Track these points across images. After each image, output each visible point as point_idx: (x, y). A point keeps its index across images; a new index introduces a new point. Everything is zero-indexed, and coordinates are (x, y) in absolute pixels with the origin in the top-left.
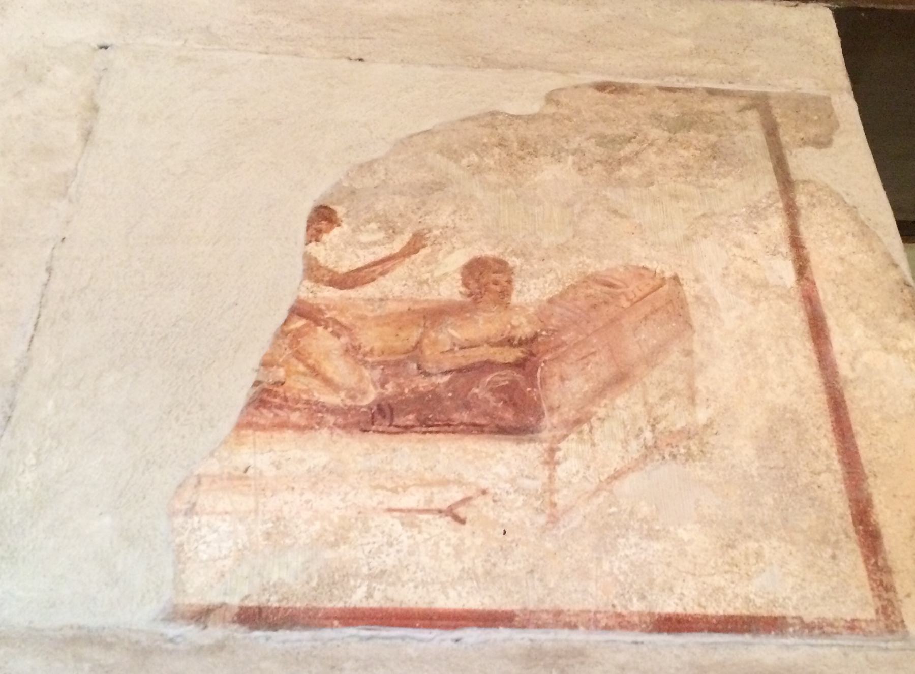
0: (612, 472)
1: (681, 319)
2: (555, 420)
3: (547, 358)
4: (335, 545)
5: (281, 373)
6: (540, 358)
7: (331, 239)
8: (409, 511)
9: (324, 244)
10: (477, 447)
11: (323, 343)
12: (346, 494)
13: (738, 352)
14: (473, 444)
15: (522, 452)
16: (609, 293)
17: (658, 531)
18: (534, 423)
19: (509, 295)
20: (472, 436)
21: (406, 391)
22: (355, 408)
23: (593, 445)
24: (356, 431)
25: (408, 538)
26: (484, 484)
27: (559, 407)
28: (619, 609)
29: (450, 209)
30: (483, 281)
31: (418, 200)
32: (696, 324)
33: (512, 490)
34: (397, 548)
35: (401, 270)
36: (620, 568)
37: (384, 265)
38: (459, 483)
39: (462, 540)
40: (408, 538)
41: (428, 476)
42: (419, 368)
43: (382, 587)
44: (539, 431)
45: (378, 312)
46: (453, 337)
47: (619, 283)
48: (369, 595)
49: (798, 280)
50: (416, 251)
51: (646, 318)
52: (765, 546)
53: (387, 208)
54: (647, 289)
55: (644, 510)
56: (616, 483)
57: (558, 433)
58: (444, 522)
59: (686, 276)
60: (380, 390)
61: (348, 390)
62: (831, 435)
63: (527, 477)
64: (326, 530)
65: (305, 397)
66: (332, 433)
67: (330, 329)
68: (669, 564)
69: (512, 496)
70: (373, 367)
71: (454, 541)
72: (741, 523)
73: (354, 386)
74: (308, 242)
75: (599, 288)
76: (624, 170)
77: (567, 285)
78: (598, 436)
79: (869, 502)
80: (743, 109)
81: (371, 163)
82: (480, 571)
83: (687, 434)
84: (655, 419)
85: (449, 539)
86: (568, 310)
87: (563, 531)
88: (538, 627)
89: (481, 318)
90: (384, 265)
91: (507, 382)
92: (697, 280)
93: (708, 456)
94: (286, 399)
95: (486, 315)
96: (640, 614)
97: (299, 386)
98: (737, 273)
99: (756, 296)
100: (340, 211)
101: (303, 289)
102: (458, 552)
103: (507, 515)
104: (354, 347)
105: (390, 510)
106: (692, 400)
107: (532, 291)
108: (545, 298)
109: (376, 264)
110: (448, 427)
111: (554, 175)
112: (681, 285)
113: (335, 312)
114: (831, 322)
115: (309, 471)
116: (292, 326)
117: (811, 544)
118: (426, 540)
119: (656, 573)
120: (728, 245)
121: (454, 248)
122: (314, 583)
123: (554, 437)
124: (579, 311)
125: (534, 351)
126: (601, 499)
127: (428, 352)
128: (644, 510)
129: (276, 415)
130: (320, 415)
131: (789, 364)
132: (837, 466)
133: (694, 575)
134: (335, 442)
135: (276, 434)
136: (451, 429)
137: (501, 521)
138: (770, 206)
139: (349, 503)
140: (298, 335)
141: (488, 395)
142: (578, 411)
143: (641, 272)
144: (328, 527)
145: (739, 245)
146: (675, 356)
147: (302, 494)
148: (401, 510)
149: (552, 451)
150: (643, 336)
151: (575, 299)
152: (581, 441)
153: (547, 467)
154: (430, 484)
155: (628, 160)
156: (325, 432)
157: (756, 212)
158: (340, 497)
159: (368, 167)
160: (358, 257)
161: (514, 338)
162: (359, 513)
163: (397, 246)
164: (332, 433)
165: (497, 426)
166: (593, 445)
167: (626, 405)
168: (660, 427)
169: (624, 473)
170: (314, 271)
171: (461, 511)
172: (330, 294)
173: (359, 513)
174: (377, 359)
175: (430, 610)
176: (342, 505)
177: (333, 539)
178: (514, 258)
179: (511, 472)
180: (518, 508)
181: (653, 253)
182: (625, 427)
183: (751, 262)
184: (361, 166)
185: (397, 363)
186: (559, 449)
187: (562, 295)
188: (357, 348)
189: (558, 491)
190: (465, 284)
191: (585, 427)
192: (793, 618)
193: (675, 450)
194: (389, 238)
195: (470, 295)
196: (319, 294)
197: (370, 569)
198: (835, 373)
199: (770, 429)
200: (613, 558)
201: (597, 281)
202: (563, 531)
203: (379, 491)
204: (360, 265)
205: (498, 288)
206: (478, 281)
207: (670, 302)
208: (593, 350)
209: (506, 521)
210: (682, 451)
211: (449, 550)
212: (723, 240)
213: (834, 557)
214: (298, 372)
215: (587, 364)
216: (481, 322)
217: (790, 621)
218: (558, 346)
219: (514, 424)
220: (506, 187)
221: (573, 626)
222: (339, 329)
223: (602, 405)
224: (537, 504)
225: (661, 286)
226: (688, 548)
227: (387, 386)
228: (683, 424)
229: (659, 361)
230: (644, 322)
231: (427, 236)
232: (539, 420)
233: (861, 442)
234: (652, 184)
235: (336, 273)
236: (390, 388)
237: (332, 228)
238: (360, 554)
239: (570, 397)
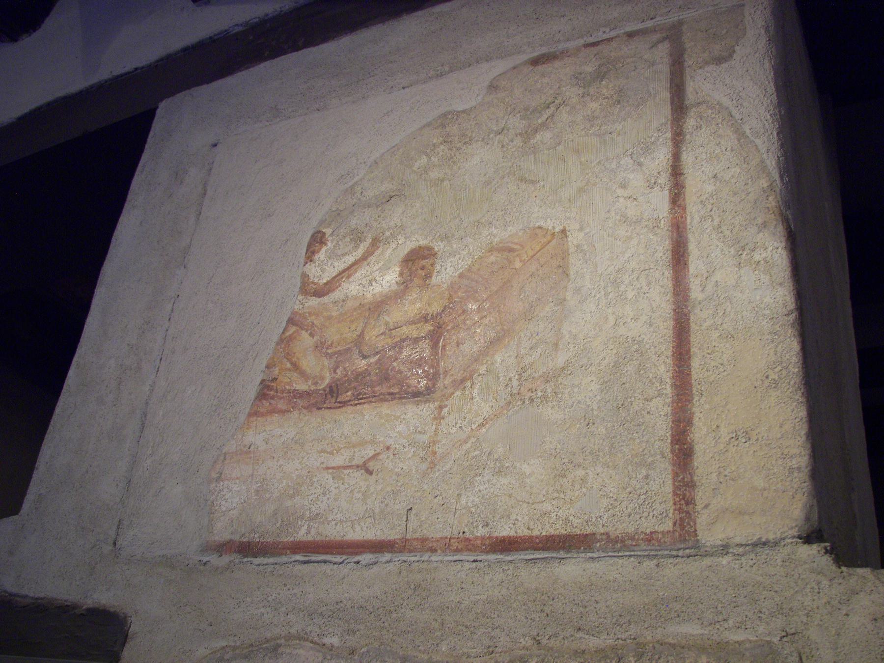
2: (448, 381)
3: (449, 328)
4: (292, 497)
8: (339, 467)
12: (303, 458)
13: (603, 293)
24: (314, 409)
26: (390, 442)
28: (467, 535)
29: (401, 211)
39: (368, 487)
41: (354, 439)
43: (316, 526)
48: (308, 532)
49: (671, 209)
54: (538, 247)
58: (358, 474)
59: (573, 226)
60: (333, 375)
62: (669, 361)
63: (420, 432)
65: (288, 387)
68: (510, 496)
76: (538, 137)
79: (690, 422)
80: (654, 45)
82: (377, 511)
85: (361, 487)
87: (437, 474)
88: (410, 551)
92: (581, 229)
93: (560, 396)
96: (483, 538)
98: (616, 214)
99: (629, 234)
100: (328, 231)
102: (365, 495)
103: (401, 465)
104: (321, 343)
109: (344, 271)
112: (566, 237)
113: (314, 317)
114: (692, 247)
115: (283, 443)
117: (630, 467)
118: (346, 489)
122: (278, 525)
126: (469, 445)
128: (500, 450)
132: (669, 390)
137: (396, 470)
140: (291, 339)
145: (623, 186)
148: (333, 468)
149: (441, 408)
154: (354, 446)
155: (544, 126)
156: (296, 413)
157: (647, 149)
168: (525, 375)
171: (371, 465)
175: (342, 541)
178: (440, 243)
186: (446, 406)
189: (439, 441)
191: (468, 384)
192: (602, 534)
196: (306, 305)
198: (686, 298)
202: (437, 474)
204: (334, 274)
210: (540, 394)
211: (360, 495)
213: (647, 477)
217: (598, 537)
220: (443, 180)
221: (433, 550)
224: (423, 454)
225: (549, 242)
226: (528, 480)
227: (338, 371)
228: (545, 370)
233: (695, 363)
234: (559, 144)
237: (321, 249)
238: (306, 503)
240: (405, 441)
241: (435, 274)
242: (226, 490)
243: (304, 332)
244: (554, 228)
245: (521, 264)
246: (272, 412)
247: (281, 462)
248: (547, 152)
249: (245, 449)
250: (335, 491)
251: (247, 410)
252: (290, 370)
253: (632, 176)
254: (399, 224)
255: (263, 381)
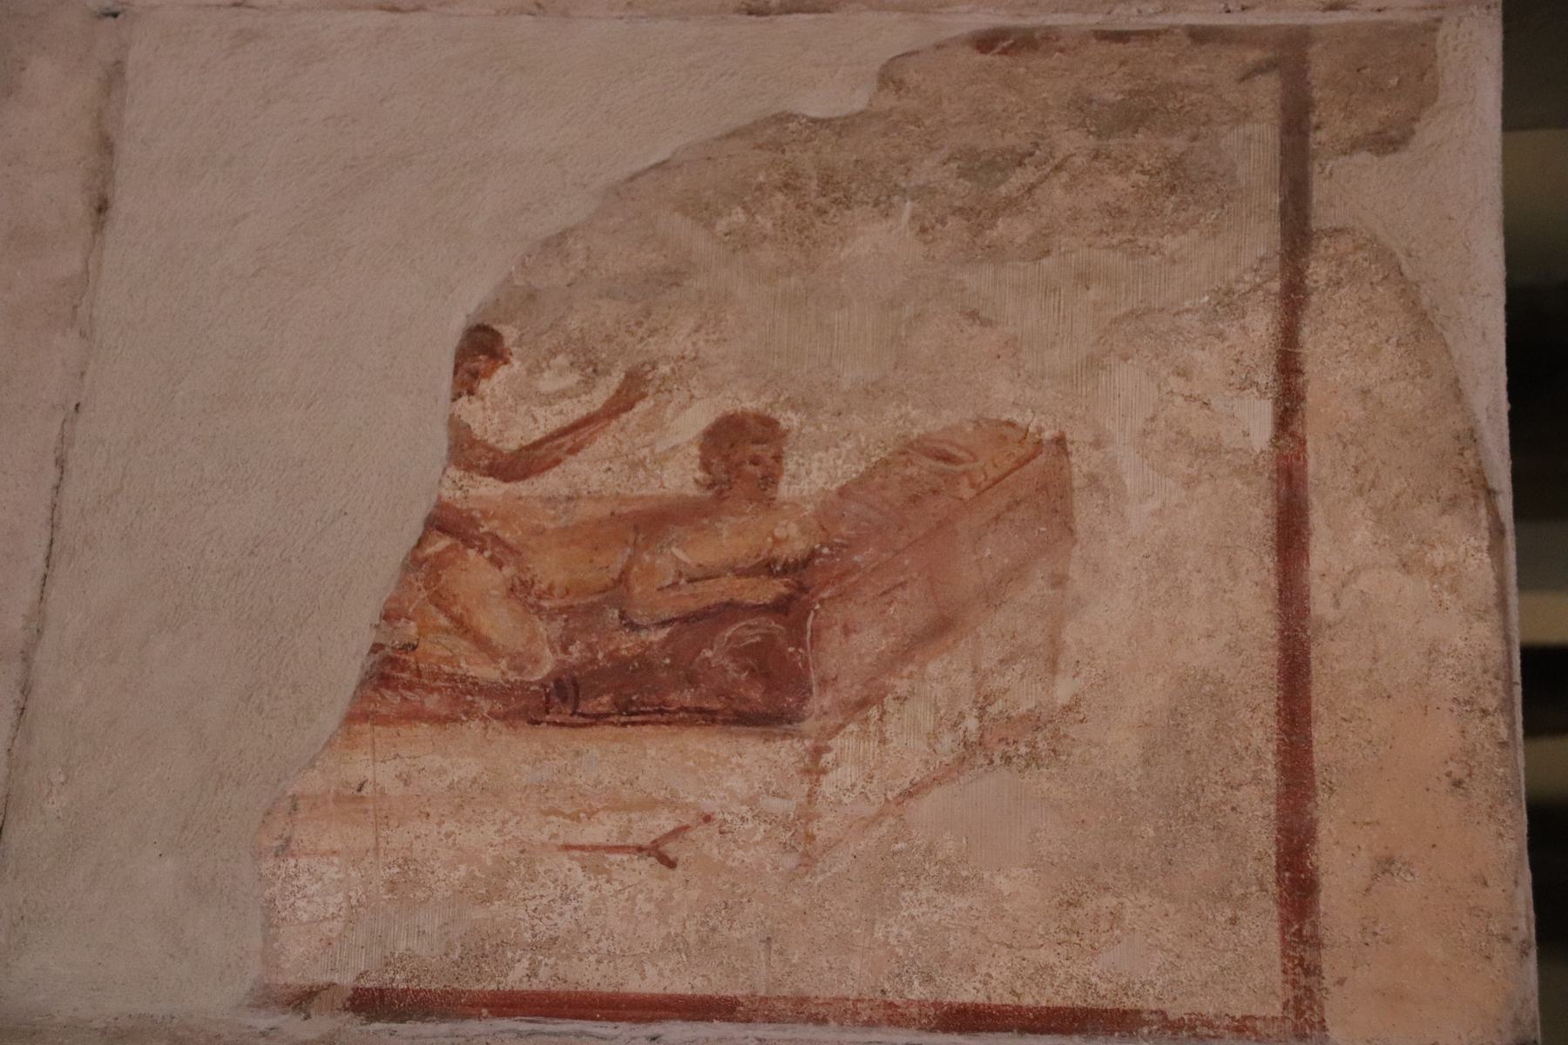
0: (907, 785)
1: (1057, 519)
2: (826, 702)
3: (825, 595)
4: (486, 900)
5: (412, 629)
6: (813, 596)
7: (493, 390)
8: (595, 848)
9: (482, 399)
10: (702, 747)
11: (477, 578)
12: (504, 822)
13: (1145, 578)
14: (697, 742)
15: (770, 755)
16: (942, 474)
17: (967, 878)
18: (794, 706)
19: (775, 483)
20: (696, 729)
21: (600, 656)
22: (524, 686)
23: (883, 741)
24: (522, 723)
25: (591, 889)
26: (708, 806)
27: (835, 679)
29: (691, 323)
30: (736, 458)
31: (638, 306)
32: (1081, 523)
33: (749, 816)
34: (574, 903)
35: (603, 443)
36: (900, 935)
37: (575, 435)
38: (672, 803)
40: (591, 889)
41: (626, 793)
42: (622, 617)
44: (802, 720)
45: (562, 522)
46: (678, 561)
47: (961, 454)
50: (631, 406)
51: (997, 518)
52: (1128, 904)
53: (586, 325)
54: (1008, 464)
55: (949, 846)
56: (912, 803)
57: (831, 722)
58: (645, 865)
59: (1078, 436)
60: (561, 656)
61: (513, 657)
63: (775, 794)
64: (474, 878)
65: (447, 669)
66: (486, 728)
67: (487, 554)
68: (974, 931)
69: (749, 826)
70: (551, 617)
71: (657, 894)
72: (1096, 867)
73: (521, 649)
74: (456, 397)
75: (928, 462)
77: (874, 460)
78: (890, 729)
81: (562, 236)
83: (1034, 721)
84: (986, 698)
86: (871, 507)
87: (820, 878)
89: (726, 526)
90: (575, 435)
91: (758, 639)
92: (1097, 444)
94: (419, 673)
95: (732, 520)
97: (440, 651)
99: (1193, 471)
100: (509, 334)
101: (447, 483)
103: (739, 853)
104: (523, 583)
105: (567, 847)
106: (1053, 666)
107: (815, 474)
108: (834, 488)
109: (563, 432)
110: (662, 715)
111: (876, 246)
112: (1068, 454)
113: (495, 523)
115: (451, 787)
116: (430, 550)
119: (953, 943)
120: (1164, 373)
121: (692, 397)
123: (823, 728)
124: (886, 508)
125: (807, 583)
127: (638, 589)
128: (949, 846)
129: (405, 699)
130: (469, 698)
131: (1228, 596)
133: (1010, 947)
134: (490, 742)
135: (404, 730)
136: (664, 719)
137: (729, 863)
138: (1254, 289)
139: (508, 837)
141: (726, 662)
142: (865, 685)
143: (1003, 432)
144: (477, 873)
145: (1183, 373)
146: (1037, 587)
147: (440, 824)
148: (582, 848)
149: (818, 752)
150: (988, 552)
151: (883, 487)
152: (864, 735)
153: (807, 780)
154: (628, 807)
156: (475, 725)
158: (495, 828)
159: (556, 244)
160: (536, 421)
161: (775, 561)
162: (522, 852)
163: (599, 397)
164: (486, 728)
165: (736, 713)
166: (883, 741)
167: (943, 676)
168: (992, 710)
169: (926, 786)
170: (467, 451)
171: (671, 849)
172: (490, 489)
173: (522, 852)
174: (559, 602)
176: (497, 839)
177: (483, 891)
178: (791, 414)
179: (751, 787)
180: (758, 843)
181: (1029, 392)
182: (938, 710)
183: (1198, 404)
184: (546, 244)
185: (592, 610)
186: (828, 749)
187: (862, 481)
188: (527, 586)
189: (819, 816)
190: (706, 466)
191: (874, 712)
193: (1011, 750)
194: (586, 383)
195: (710, 486)
196: (472, 492)
197: (534, 936)
199: (1173, 712)
200: (891, 921)
201: (928, 453)
202: (820, 878)
203: (553, 818)
204: (537, 436)
205: (758, 471)
206: (726, 458)
207: (1043, 488)
208: (902, 579)
209: (736, 864)
210: (1023, 750)
212: (1154, 363)
214: (438, 629)
215: (890, 604)
216: (725, 533)
218: (847, 573)
219: (762, 709)
222: (501, 552)
223: (905, 673)
225: (1034, 457)
226: (1007, 906)
227: (572, 649)
228: (1032, 705)
229: (1008, 595)
230: (993, 527)
231: (650, 376)
232: (803, 700)
234: (1047, 253)
235: (500, 452)
236: (576, 650)
237: (493, 370)
238: (521, 913)
239: (855, 661)
240: (745, 808)
241: (785, 478)
242: (303, 879)
243: (472, 553)
244: (1040, 430)
245: (973, 492)
246: (415, 716)
247: (449, 826)
248: (1022, 264)
249: (349, 792)
250: (589, 896)
251: (341, 705)
252: (447, 631)
253: (1200, 355)
254: (690, 353)
255: (376, 648)
